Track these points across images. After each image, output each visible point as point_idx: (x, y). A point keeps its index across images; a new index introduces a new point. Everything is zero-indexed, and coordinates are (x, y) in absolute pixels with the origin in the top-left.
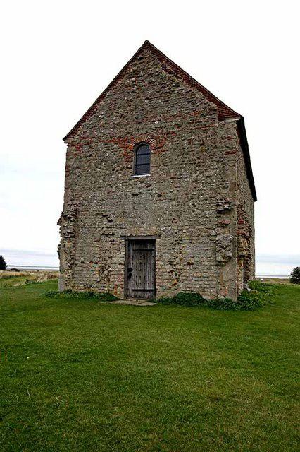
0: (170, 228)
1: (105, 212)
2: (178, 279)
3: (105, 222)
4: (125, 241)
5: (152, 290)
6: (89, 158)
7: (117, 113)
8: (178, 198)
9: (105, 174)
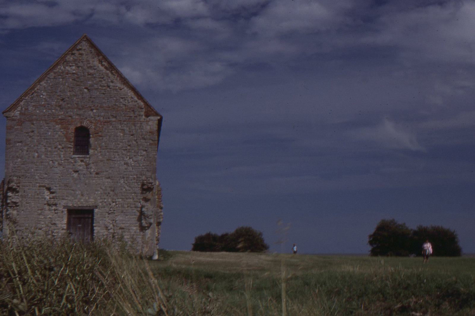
1: (48, 184)
3: (47, 193)
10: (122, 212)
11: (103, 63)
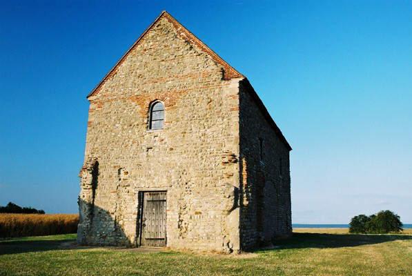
5: (164, 239)
9: (123, 129)
11: (182, 34)
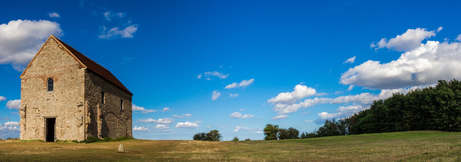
0: (61, 113)
2: (64, 133)
4: (45, 119)
6: (30, 85)
7: (40, 65)
8: (64, 101)
10: (68, 118)
11: (60, 46)
